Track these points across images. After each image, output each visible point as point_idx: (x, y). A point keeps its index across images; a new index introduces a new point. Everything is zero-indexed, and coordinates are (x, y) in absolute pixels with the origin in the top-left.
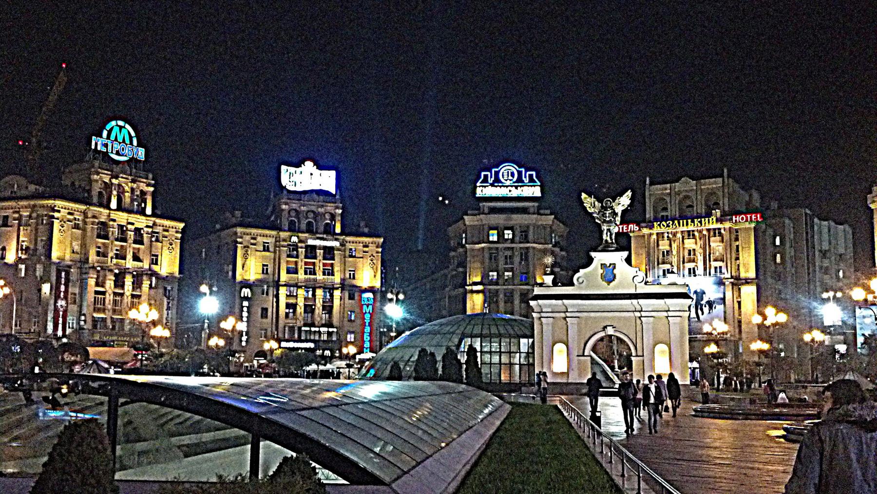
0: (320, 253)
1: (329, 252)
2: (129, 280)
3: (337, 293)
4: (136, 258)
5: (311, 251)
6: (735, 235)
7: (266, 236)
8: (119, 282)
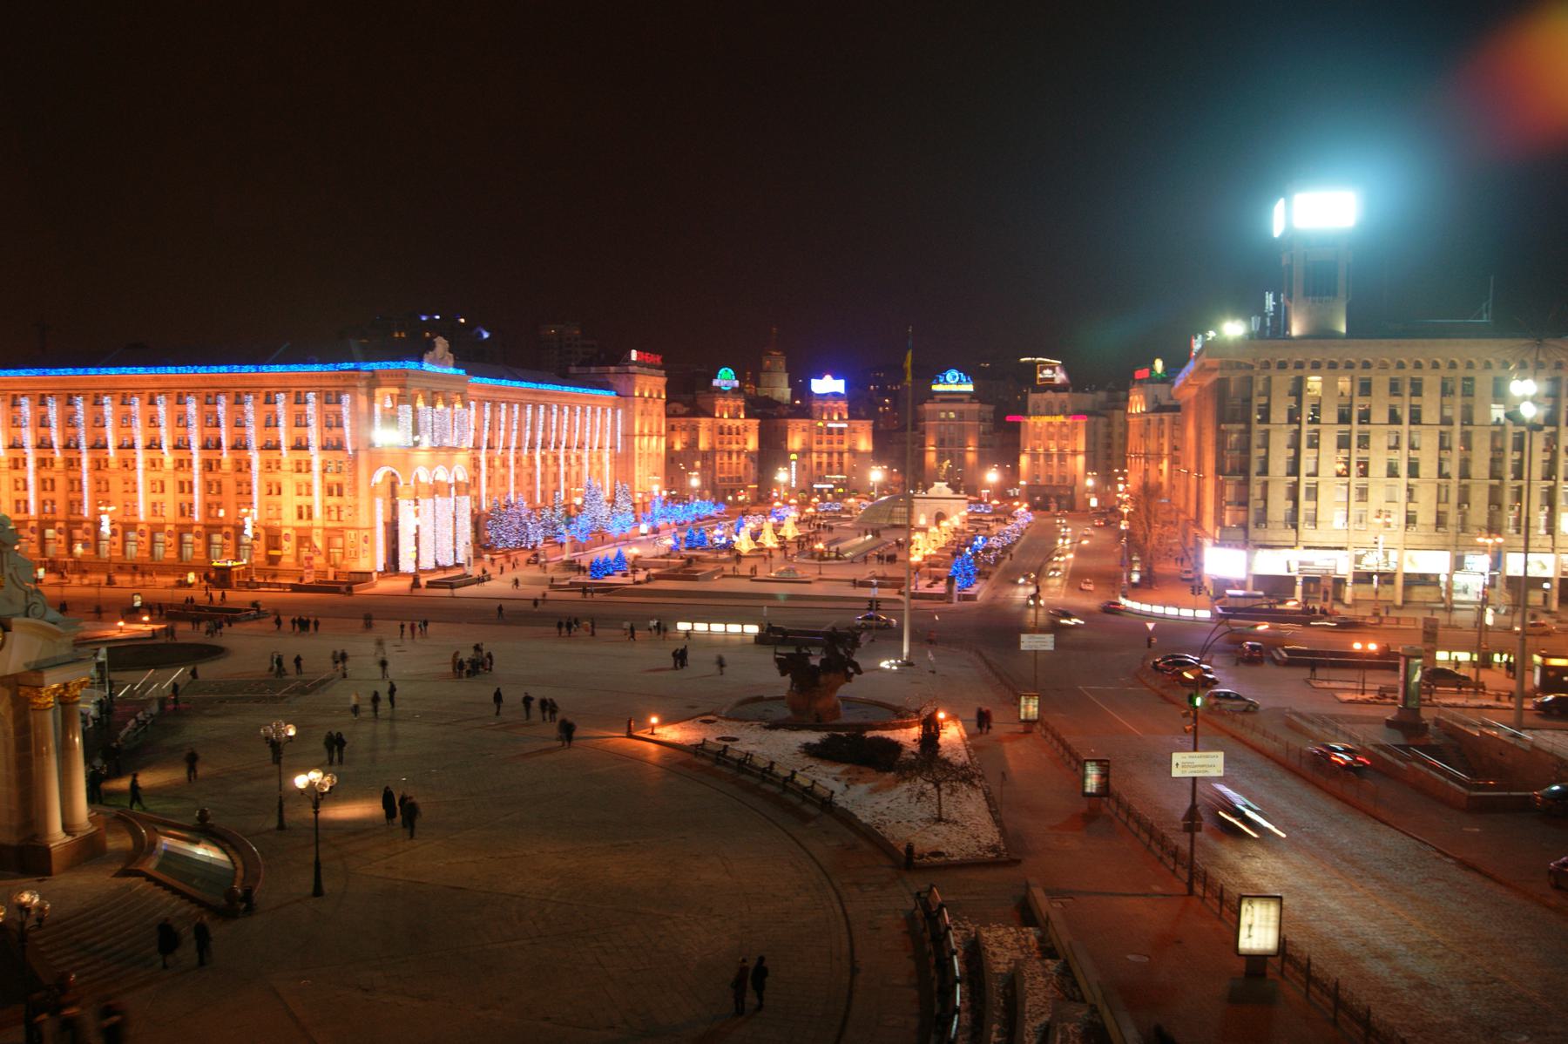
1: (841, 431)
2: (734, 457)
3: (846, 455)
5: (830, 431)
6: (1075, 426)
7: (803, 423)
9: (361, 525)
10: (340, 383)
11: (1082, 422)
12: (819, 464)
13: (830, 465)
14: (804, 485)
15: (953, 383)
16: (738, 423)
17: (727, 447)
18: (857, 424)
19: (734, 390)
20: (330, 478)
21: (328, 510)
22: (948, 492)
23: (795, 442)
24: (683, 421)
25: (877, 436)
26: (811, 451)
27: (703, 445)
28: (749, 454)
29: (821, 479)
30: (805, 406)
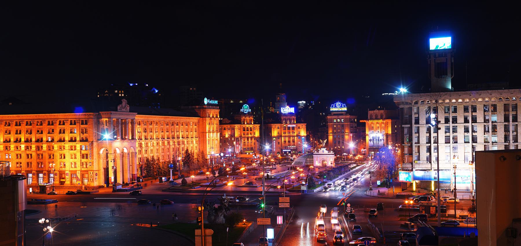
0: (291, 128)
1: (293, 128)
2: (250, 140)
3: (296, 138)
4: (251, 134)
5: (289, 128)
6: (387, 124)
7: (278, 125)
8: (248, 140)
9: (95, 169)
10: (87, 117)
11: (389, 121)
12: (285, 141)
13: (289, 142)
14: (279, 150)
15: (338, 107)
16: (251, 126)
17: (247, 136)
18: (300, 125)
19: (249, 112)
20: (83, 152)
21: (82, 164)
22: (326, 152)
23: (275, 133)
24: (229, 126)
25: (307, 130)
26: (281, 136)
27: (237, 135)
28: (255, 138)
29: (286, 148)
30: (278, 118)
